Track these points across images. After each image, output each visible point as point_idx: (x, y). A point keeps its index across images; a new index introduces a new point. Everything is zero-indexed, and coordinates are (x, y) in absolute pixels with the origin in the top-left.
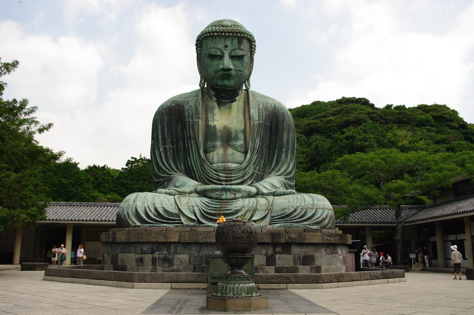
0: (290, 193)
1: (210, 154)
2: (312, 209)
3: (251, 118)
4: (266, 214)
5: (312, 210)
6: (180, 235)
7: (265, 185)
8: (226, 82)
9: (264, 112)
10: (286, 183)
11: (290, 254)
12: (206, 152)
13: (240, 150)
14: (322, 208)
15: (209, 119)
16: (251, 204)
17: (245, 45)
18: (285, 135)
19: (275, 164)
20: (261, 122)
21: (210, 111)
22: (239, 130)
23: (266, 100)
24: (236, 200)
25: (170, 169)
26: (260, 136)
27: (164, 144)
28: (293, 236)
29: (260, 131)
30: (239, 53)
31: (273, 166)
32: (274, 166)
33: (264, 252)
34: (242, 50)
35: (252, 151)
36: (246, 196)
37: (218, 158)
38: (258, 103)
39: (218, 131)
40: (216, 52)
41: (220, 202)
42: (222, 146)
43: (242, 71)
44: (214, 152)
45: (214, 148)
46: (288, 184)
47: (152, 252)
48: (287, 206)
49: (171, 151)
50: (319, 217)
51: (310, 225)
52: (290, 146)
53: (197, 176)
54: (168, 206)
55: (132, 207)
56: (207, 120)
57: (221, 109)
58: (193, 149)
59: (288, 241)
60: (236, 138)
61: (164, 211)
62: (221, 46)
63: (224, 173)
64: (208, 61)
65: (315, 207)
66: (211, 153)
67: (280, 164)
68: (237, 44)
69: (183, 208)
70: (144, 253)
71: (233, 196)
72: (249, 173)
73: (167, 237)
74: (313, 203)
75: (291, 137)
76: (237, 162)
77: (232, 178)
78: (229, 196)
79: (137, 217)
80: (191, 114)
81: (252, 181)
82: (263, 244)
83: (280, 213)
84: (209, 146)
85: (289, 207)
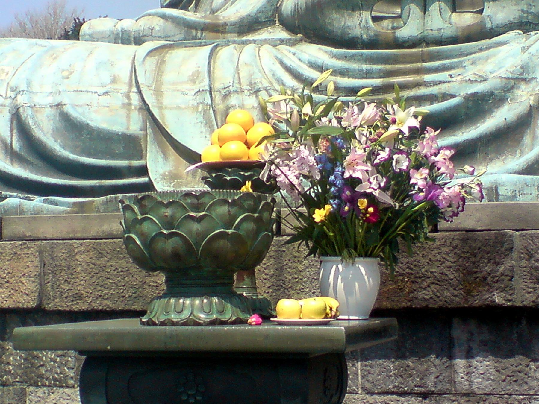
24: (487, 41)
41: (385, 60)
54: (85, 98)
69: (167, 101)
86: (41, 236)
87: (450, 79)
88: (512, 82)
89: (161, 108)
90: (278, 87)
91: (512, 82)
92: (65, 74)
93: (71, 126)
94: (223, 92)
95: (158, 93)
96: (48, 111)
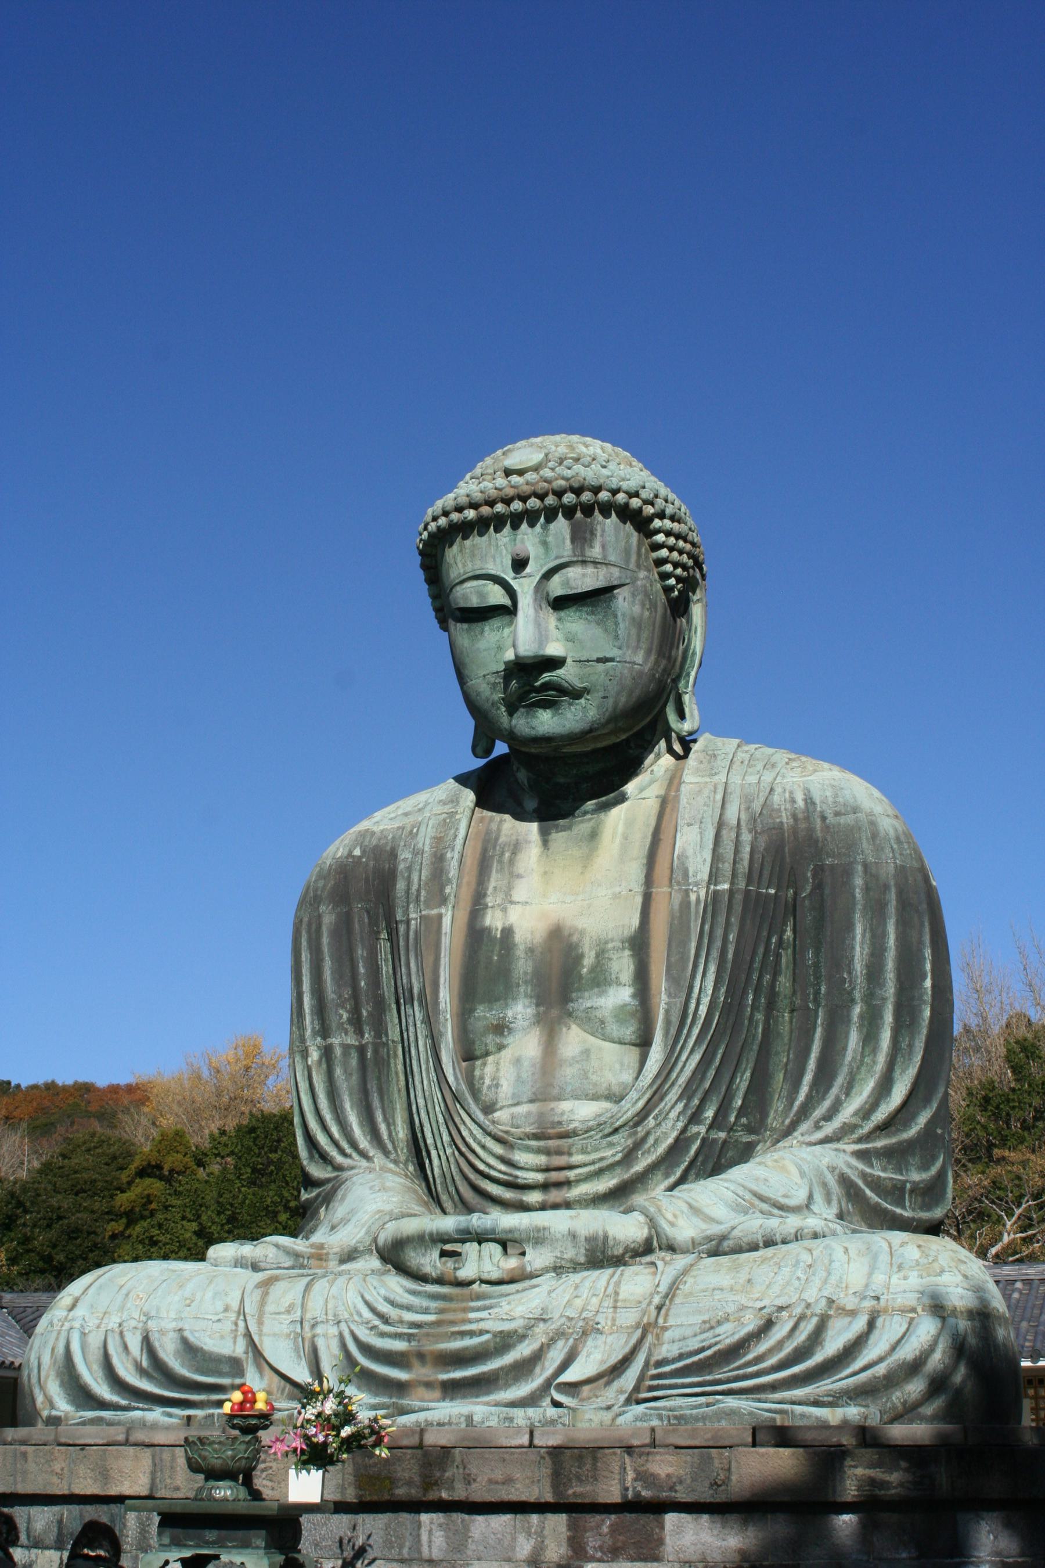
0: (797, 1237)
1: (484, 1064)
2: (853, 1313)
3: (678, 876)
4: (627, 1350)
5: (850, 1323)
6: (155, 1465)
8: (546, 722)
9: (746, 837)
10: (864, 1176)
11: (656, 1559)
13: (616, 1034)
14: (903, 1311)
15: (490, 900)
16: (578, 1303)
18: (858, 938)
19: (815, 1084)
20: (726, 886)
21: (500, 862)
22: (612, 940)
23: (768, 777)
25: (345, 1145)
26: (715, 954)
27: (324, 1032)
28: (664, 1466)
29: (719, 932)
30: (581, 579)
31: (802, 1096)
32: (809, 1097)
33: (524, 1548)
34: (595, 563)
35: (673, 1031)
36: (582, 1259)
37: (518, 1078)
38: (719, 797)
39: (520, 952)
40: (482, 595)
42: (539, 1020)
43: (611, 660)
44: (503, 1053)
45: (502, 1034)
46: (875, 1184)
48: (731, 1308)
49: (354, 1062)
50: (881, 1359)
51: (816, 1403)
52: (890, 989)
53: (437, 1171)
55: (59, 1333)
57: (552, 845)
58: (421, 1043)
59: (638, 1494)
60: (600, 979)
61: (180, 1347)
63: (539, 1151)
65: (868, 1304)
66: (490, 1059)
67: (840, 1080)
68: (568, 542)
70: (36, 1546)
71: (512, 1263)
72: (656, 1141)
73: (105, 1475)
74: (867, 1286)
75: (891, 941)
76: (602, 1090)
77: (572, 1174)
79: (66, 1378)
80: (415, 887)
81: (672, 1179)
83: (694, 1344)
84: (480, 1025)
85: (741, 1314)
86: (156, 1442)
87: (488, 1316)
88: (533, 1322)
89: (260, 1335)
90: (356, 1318)
91: (533, 1322)
92: (188, 1302)
93: (189, 1349)
94: (312, 1322)
95: (260, 1323)
96: (172, 1335)
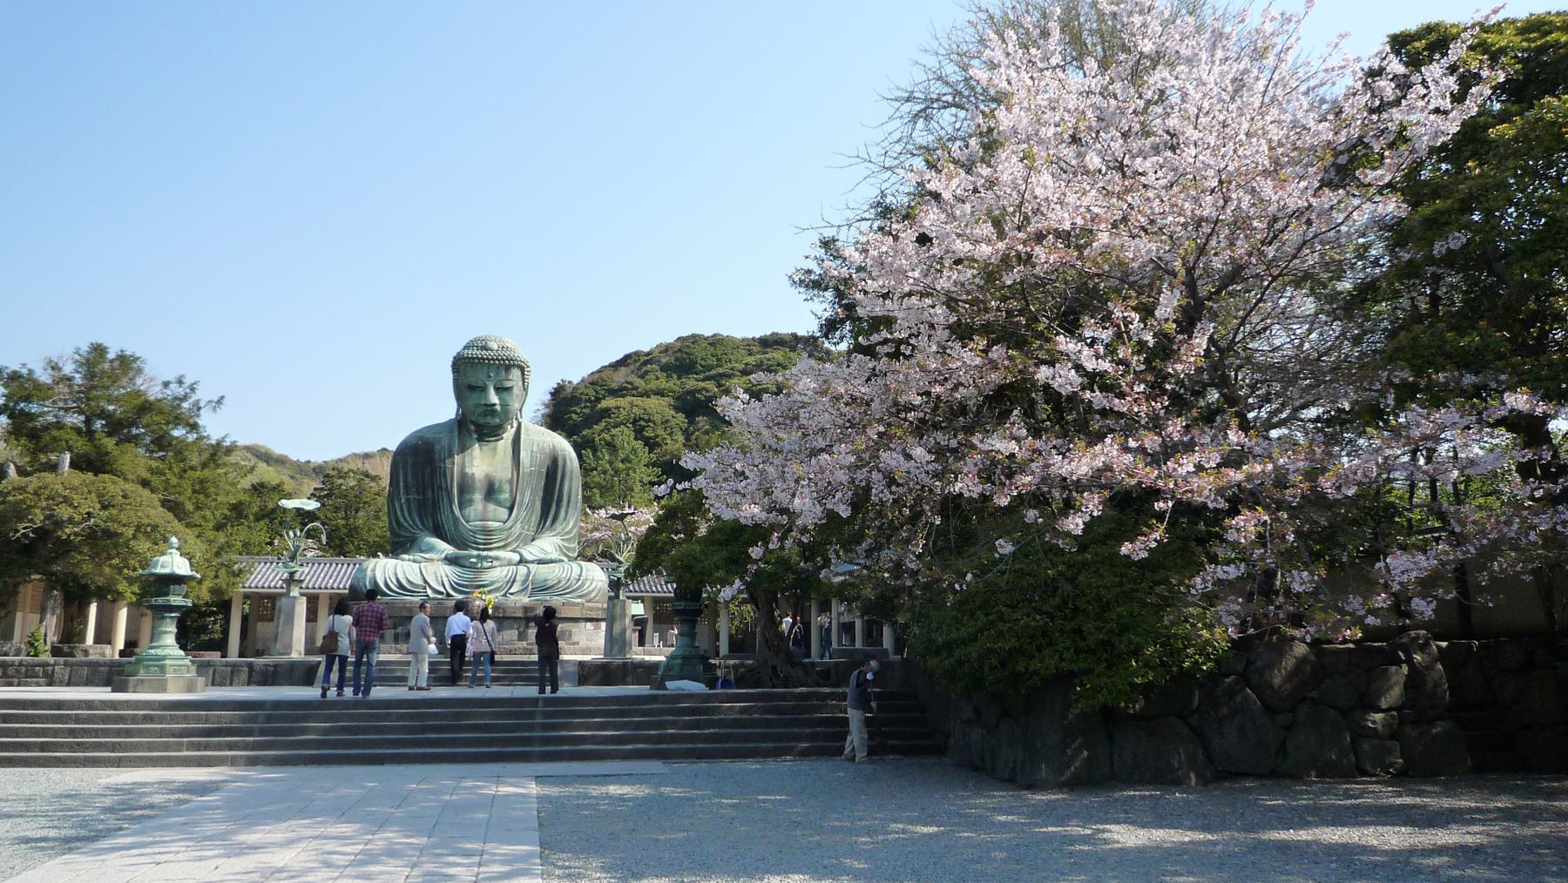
7: (531, 552)
12: (461, 507)
17: (516, 373)
27: (407, 493)
47: (395, 627)
56: (463, 466)
62: (482, 376)
64: (467, 393)
78: (486, 564)
82: (515, 618)
